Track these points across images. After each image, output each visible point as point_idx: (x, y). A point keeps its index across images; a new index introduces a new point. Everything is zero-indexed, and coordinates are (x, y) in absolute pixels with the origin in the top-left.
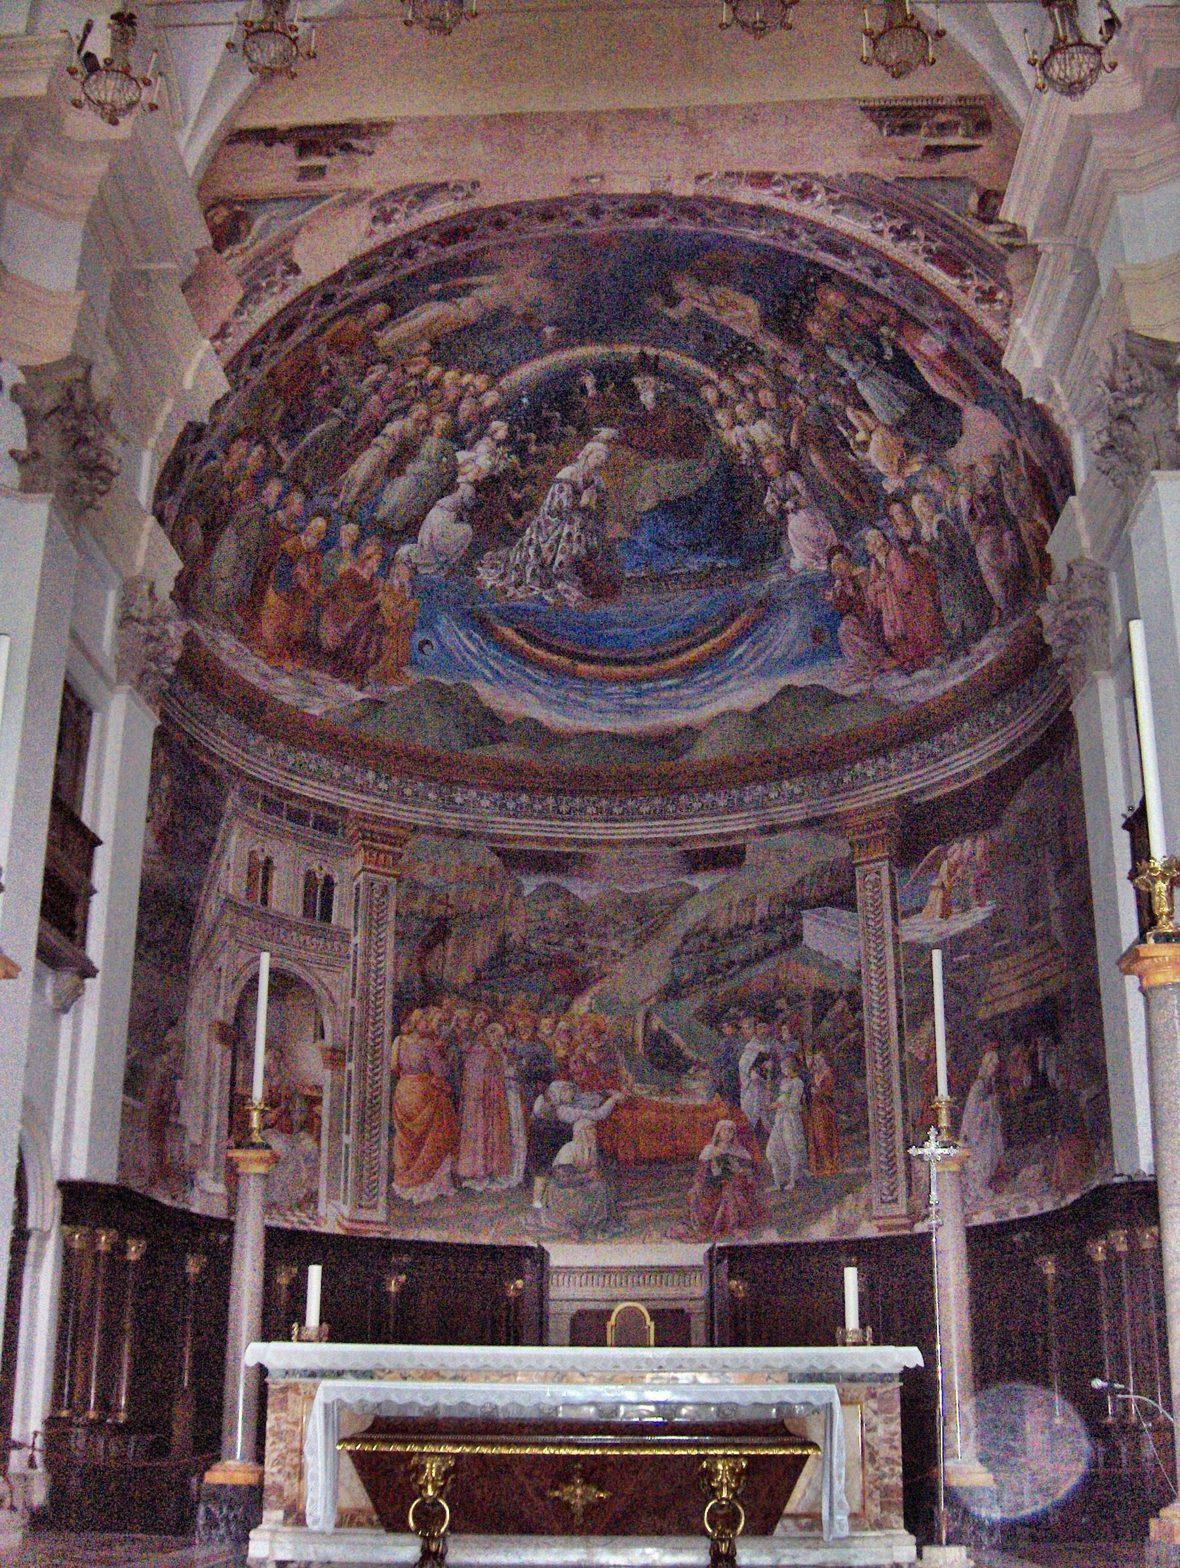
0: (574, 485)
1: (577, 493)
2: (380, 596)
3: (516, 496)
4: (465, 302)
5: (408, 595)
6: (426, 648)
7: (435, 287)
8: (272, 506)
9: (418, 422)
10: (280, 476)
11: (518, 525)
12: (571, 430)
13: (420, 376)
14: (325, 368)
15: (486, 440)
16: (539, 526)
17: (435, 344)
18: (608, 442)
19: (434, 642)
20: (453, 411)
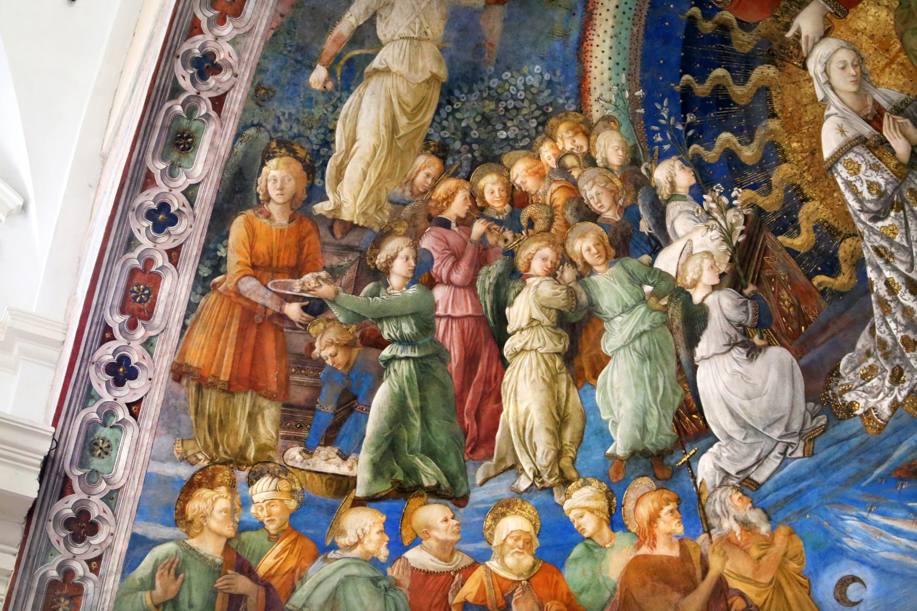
0: (861, 141)
1: (879, 146)
2: (716, 564)
3: (801, 241)
4: (384, 57)
5: (764, 529)
6: (853, 592)
7: (318, 76)
8: (383, 554)
9: (552, 274)
10: (358, 503)
11: (843, 281)
12: (764, 72)
13: (478, 208)
14: (293, 310)
15: (673, 209)
16: (876, 250)
17: (442, 152)
18: (827, 33)
19: (857, 571)
20: (588, 215)
